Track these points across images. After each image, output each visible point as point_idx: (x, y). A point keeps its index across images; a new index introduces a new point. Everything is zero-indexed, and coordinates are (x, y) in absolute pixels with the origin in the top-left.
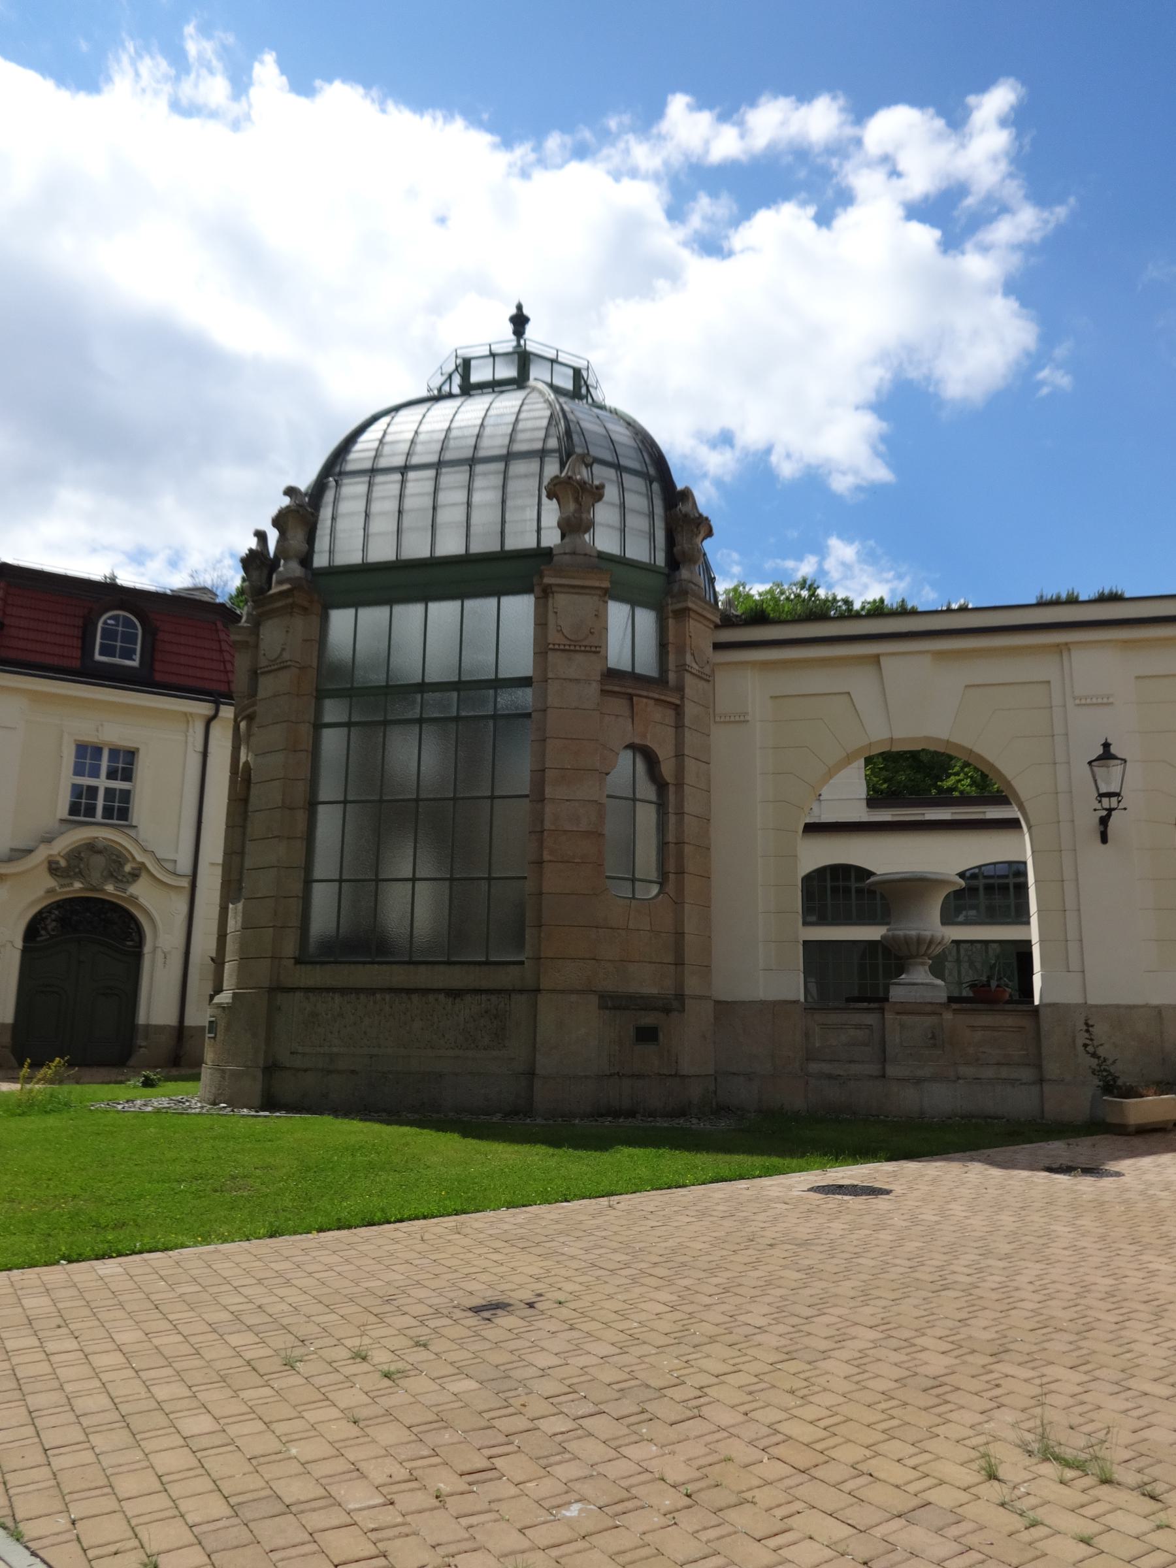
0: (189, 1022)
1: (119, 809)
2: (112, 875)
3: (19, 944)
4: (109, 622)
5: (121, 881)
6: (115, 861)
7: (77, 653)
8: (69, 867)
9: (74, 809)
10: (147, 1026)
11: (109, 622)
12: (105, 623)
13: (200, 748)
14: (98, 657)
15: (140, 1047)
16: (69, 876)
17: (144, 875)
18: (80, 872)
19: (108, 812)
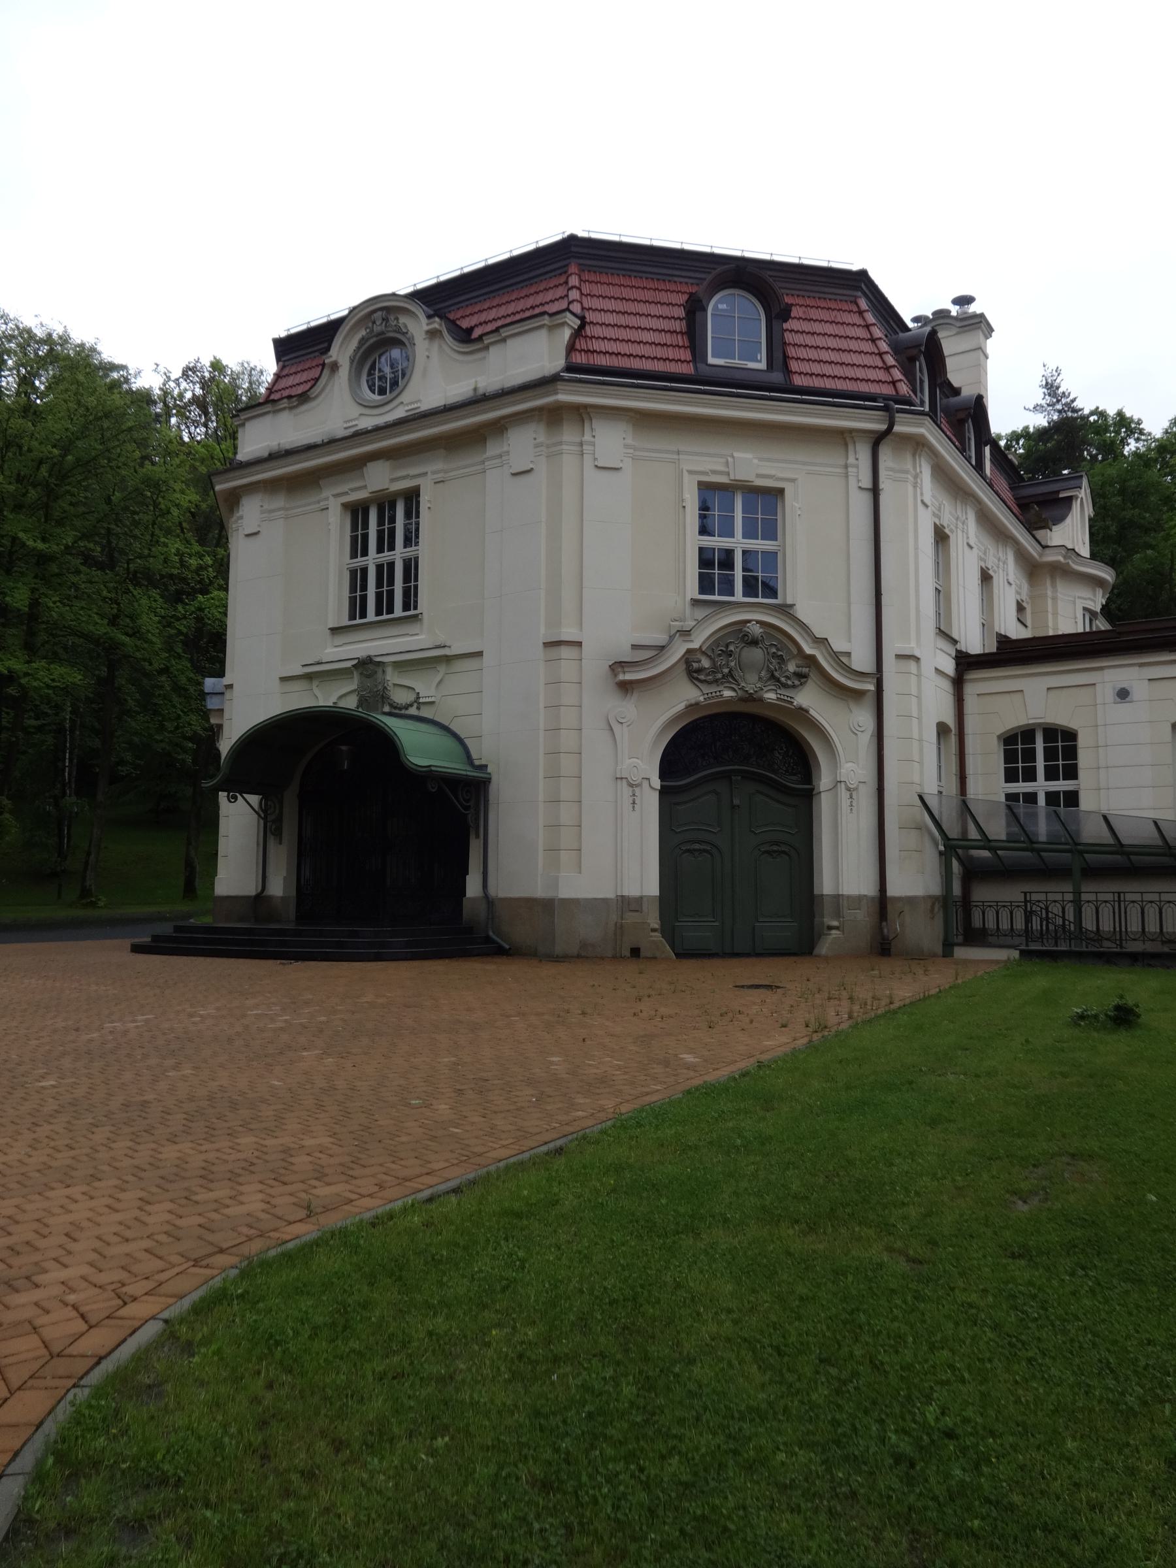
0: (892, 891)
1: (762, 585)
2: (773, 677)
3: (657, 783)
4: (720, 306)
5: (785, 686)
6: (774, 655)
7: (686, 355)
8: (715, 669)
9: (705, 584)
10: (838, 897)
11: (720, 306)
12: (715, 308)
13: (867, 482)
14: (711, 360)
15: (830, 928)
16: (716, 681)
18: (730, 674)
19: (750, 587)
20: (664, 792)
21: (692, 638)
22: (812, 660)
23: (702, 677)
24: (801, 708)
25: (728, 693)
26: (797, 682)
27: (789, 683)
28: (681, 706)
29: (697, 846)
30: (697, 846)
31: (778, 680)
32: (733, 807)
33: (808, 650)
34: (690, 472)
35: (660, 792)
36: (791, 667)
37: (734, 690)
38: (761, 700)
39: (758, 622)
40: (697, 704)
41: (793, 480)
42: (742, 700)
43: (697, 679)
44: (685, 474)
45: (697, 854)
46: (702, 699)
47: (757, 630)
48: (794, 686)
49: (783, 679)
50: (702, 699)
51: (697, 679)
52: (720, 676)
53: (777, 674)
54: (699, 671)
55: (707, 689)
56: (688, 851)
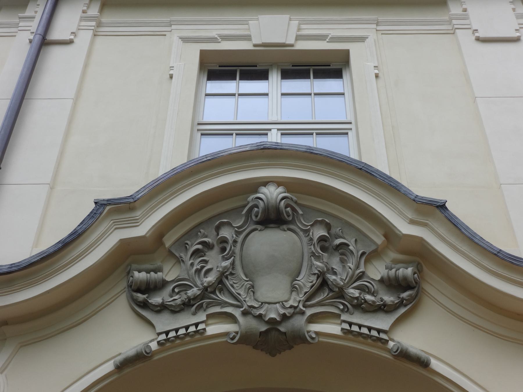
17: (434, 287)
22: (421, 255)
24: (404, 355)
25: (213, 329)
26: (389, 299)
28: (109, 367)
31: (340, 294)
34: (185, 40)
36: (377, 271)
37: (232, 318)
38: (299, 338)
40: (140, 358)
41: (362, 39)
42: (246, 339)
46: (154, 346)
47: (272, 193)
48: (383, 309)
50: (154, 346)
51: (145, 305)
54: (150, 288)
55: (165, 323)
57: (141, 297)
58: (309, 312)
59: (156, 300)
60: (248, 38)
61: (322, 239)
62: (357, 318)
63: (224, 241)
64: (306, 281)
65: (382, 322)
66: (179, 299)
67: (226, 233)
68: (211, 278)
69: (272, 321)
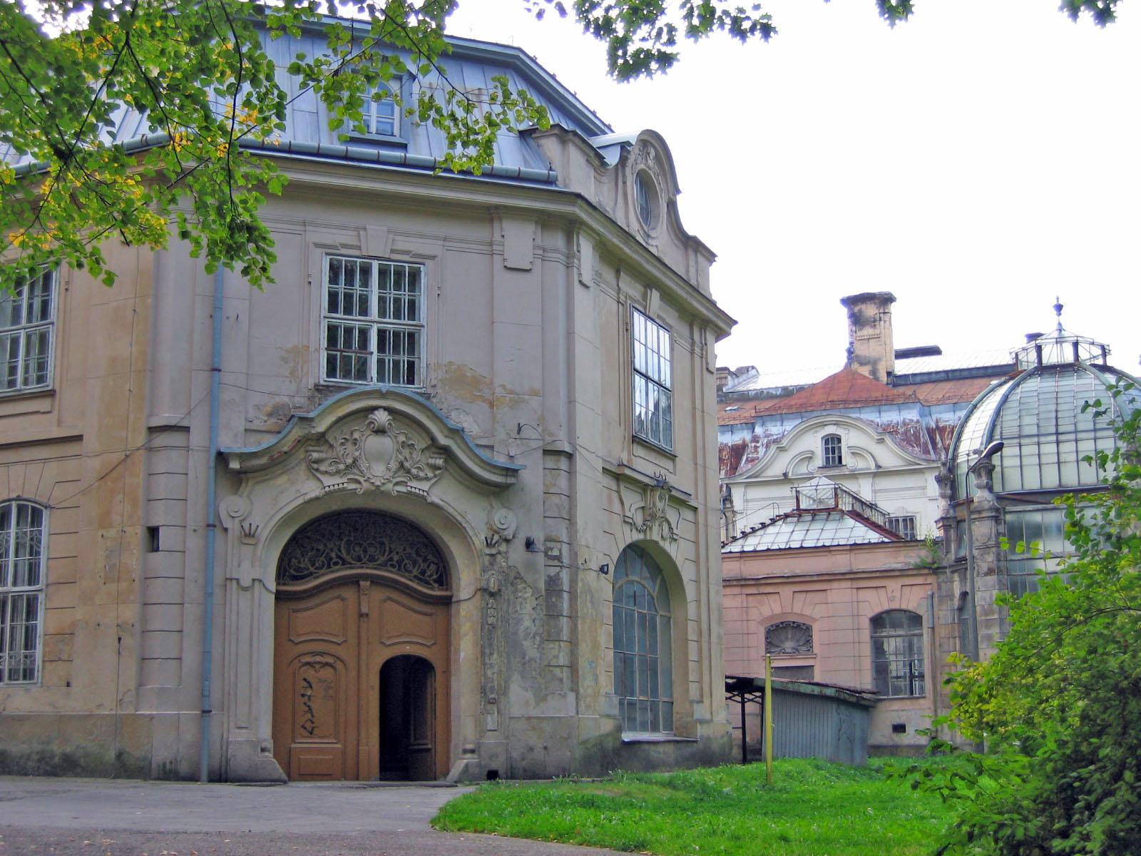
3: (273, 586)
16: (338, 472)
20: (280, 597)
21: (314, 424)
23: (323, 468)
26: (430, 475)
27: (422, 474)
29: (318, 659)
30: (318, 659)
31: (408, 472)
32: (361, 615)
33: (443, 441)
35: (277, 598)
39: (385, 409)
42: (367, 494)
43: (317, 470)
44: (312, 246)
45: (317, 666)
49: (414, 471)
51: (317, 470)
52: (342, 467)
53: (407, 464)
56: (308, 664)
57: (315, 466)
58: (395, 481)
59: (323, 468)
60: (359, 248)
61: (403, 442)
62: (414, 484)
63: (356, 439)
64: (394, 465)
65: (425, 486)
66: (333, 469)
67: (356, 435)
68: (349, 461)
69: (378, 486)
